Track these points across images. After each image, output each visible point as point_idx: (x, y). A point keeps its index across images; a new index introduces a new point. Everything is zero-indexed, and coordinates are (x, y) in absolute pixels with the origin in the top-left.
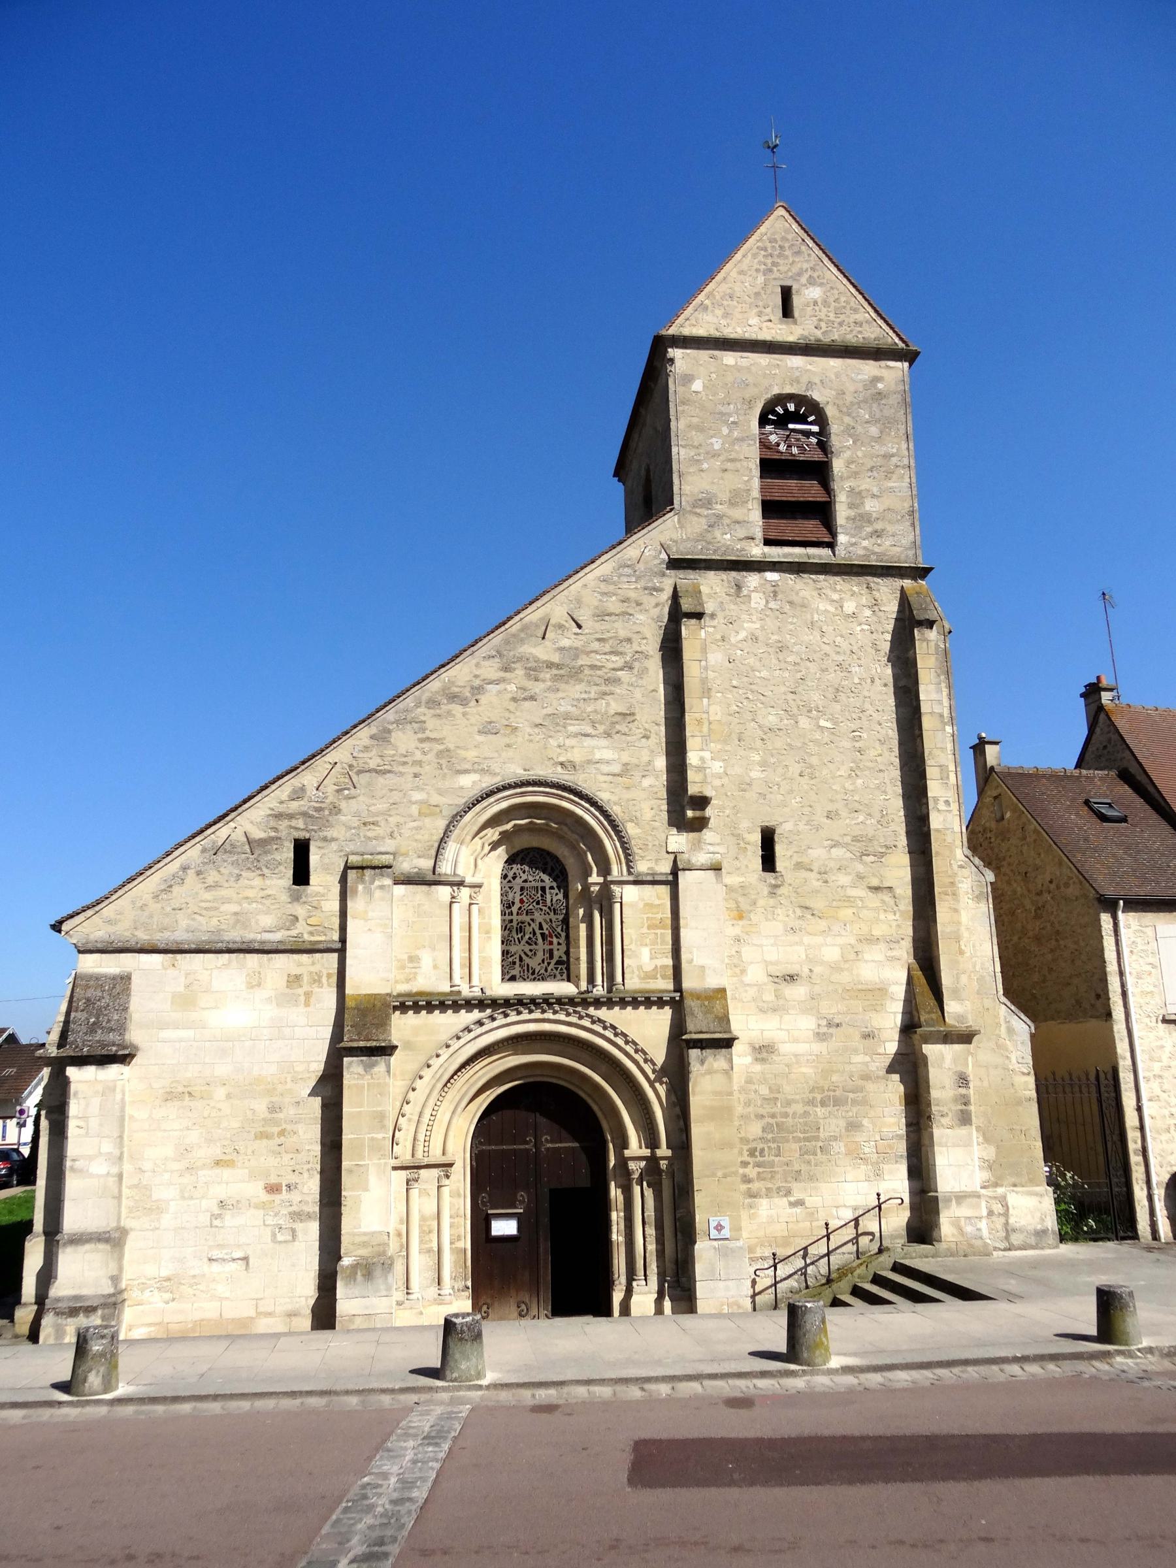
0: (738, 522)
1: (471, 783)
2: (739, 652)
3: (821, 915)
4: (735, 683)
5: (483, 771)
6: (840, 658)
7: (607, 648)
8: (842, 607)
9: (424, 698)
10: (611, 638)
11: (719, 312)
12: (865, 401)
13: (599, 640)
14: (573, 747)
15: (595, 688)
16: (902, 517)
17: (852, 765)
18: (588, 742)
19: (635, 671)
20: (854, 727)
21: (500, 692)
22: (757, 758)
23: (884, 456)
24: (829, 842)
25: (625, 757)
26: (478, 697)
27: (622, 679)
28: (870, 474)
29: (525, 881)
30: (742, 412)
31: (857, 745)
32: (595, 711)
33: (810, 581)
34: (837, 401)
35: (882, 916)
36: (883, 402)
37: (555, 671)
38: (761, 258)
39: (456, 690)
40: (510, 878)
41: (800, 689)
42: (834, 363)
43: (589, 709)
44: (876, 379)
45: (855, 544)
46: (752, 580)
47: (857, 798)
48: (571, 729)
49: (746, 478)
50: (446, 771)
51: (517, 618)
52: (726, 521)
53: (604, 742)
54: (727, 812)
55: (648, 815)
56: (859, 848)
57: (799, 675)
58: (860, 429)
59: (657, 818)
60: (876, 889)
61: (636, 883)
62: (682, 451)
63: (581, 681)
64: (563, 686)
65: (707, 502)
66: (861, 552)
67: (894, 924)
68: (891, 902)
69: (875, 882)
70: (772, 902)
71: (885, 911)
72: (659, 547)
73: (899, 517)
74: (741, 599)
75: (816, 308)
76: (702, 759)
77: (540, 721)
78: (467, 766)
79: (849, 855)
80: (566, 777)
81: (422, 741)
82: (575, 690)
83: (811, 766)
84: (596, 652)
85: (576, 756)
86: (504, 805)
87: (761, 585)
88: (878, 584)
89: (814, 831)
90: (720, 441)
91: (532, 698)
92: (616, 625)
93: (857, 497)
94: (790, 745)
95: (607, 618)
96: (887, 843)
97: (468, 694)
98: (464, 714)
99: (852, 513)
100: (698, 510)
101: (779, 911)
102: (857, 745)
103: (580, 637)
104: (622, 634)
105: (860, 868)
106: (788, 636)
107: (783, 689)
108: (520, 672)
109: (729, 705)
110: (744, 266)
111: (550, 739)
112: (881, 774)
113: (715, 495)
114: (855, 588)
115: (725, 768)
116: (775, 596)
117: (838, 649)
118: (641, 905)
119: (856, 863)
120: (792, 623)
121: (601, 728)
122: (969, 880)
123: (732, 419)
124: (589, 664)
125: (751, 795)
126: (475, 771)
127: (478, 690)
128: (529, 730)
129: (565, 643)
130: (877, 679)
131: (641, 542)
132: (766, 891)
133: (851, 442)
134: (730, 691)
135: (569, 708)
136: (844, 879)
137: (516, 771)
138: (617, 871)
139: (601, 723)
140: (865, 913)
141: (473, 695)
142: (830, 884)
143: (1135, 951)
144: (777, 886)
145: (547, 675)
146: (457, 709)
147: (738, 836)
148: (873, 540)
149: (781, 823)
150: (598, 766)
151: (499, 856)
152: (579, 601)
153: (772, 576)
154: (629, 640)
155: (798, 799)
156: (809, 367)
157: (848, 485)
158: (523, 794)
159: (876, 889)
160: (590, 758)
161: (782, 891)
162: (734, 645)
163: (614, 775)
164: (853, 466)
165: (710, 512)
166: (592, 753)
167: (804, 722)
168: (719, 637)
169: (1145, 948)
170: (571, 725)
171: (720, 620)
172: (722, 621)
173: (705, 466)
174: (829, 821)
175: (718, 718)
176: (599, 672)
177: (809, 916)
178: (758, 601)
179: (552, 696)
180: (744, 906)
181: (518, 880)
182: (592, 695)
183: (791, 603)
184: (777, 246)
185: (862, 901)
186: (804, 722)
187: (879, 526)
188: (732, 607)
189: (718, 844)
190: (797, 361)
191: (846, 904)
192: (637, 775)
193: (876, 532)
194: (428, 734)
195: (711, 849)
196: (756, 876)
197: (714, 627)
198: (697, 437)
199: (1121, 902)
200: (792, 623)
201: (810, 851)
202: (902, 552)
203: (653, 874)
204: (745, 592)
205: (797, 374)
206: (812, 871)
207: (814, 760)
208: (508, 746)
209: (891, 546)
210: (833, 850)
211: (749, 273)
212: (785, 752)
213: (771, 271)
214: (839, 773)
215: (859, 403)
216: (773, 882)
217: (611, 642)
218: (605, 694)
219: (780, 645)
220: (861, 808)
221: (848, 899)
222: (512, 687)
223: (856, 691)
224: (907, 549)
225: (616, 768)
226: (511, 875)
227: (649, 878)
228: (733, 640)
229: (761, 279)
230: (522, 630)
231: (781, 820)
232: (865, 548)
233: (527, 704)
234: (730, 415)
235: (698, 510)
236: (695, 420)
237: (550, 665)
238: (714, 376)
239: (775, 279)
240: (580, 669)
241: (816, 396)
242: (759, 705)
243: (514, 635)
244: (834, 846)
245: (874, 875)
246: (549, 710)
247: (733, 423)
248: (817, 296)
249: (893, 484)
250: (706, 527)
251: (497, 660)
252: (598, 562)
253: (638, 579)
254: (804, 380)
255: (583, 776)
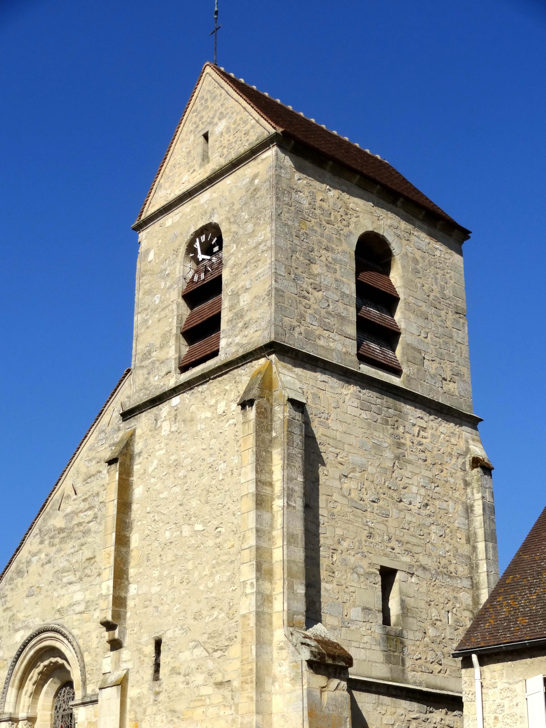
0: (163, 362)
1: (20, 637)
2: (153, 480)
3: (182, 717)
4: (148, 509)
5: (27, 627)
6: (210, 460)
7: (87, 507)
8: (216, 409)
9: (9, 578)
10: (89, 496)
11: (167, 185)
12: (246, 204)
13: (84, 500)
14: (64, 595)
15: (79, 541)
16: (263, 300)
17: (214, 562)
18: (72, 588)
19: (98, 520)
20: (216, 523)
21: (38, 561)
22: (156, 574)
23: (255, 248)
24: (193, 644)
25: (88, 597)
26: (28, 568)
27: (92, 530)
28: (245, 270)
29: (64, 710)
30: (172, 263)
31: (218, 541)
32: (77, 562)
33: (199, 395)
34: (229, 215)
35: (222, 713)
36: (257, 196)
37: (62, 535)
38: (194, 120)
39: (21, 566)
40: (58, 709)
41: (185, 501)
42: (228, 181)
43: (74, 561)
44: (255, 176)
45: (231, 343)
46: (164, 409)
47: (214, 595)
48: (65, 580)
49: (170, 320)
50: (11, 631)
51: (50, 498)
52: (157, 364)
53: (76, 587)
54: (136, 629)
55: (94, 642)
56: (213, 645)
57: (185, 487)
58: (241, 232)
59: (99, 645)
60: (219, 685)
61: (84, 704)
62: (139, 316)
63: (72, 538)
64: (63, 546)
65: (147, 355)
66: (233, 349)
67: (230, 718)
68: (228, 694)
69: (219, 678)
70: (155, 708)
71: (225, 706)
72: (120, 407)
73: (261, 302)
74: (157, 432)
75: (222, 139)
76: (108, 588)
77: (51, 579)
78: (20, 625)
79: (205, 653)
80: (59, 622)
81: (5, 610)
82: (69, 547)
83: (188, 572)
84: (81, 511)
85: (64, 603)
86: (32, 653)
87: (169, 412)
88: (240, 375)
89: (185, 634)
90: (159, 295)
91: (49, 562)
92: (94, 484)
93: (236, 295)
94: (176, 555)
95: (89, 480)
96: (231, 635)
97: (25, 568)
98: (22, 584)
99: (230, 315)
100: (143, 364)
101: (158, 718)
102: (218, 541)
103: (76, 502)
104: (96, 489)
105: (210, 665)
106: (181, 453)
107: (176, 503)
108: (47, 542)
109: (144, 530)
110: (183, 136)
111: (55, 593)
112: (232, 566)
113: (153, 345)
114: (227, 388)
115: (138, 589)
116: (176, 419)
117: (212, 452)
118: (86, 724)
119: (208, 661)
120: (184, 440)
121: (78, 574)
122: (287, 661)
123: (167, 273)
124: (77, 523)
125: (151, 609)
126: (22, 628)
127: (29, 562)
128: (46, 587)
129: (69, 510)
130: (235, 470)
131: (111, 407)
132: (152, 697)
133: (235, 247)
134: (145, 517)
135: (66, 564)
136: (199, 678)
137: (37, 623)
138: (79, 695)
139: (78, 571)
140: (212, 711)
141: (27, 567)
142: (191, 685)
143: (500, 717)
144: (157, 694)
145: (57, 541)
146: (19, 580)
147: (139, 651)
148: (242, 334)
149: (166, 632)
150: (74, 608)
151: (46, 692)
152: (78, 472)
153: (175, 401)
154: (98, 494)
155: (178, 606)
156: (215, 195)
157: (230, 290)
158: (41, 640)
159: (219, 685)
160: (71, 602)
161: (161, 697)
162: (150, 475)
163: (81, 613)
164: (234, 270)
165: (150, 361)
166: (72, 597)
167: (186, 530)
168: (142, 471)
169: (514, 710)
170: (65, 576)
171: (144, 455)
172: (146, 456)
173: (150, 322)
174: (195, 623)
175: (136, 545)
176: (81, 528)
177: (176, 720)
178: (166, 427)
179: (58, 556)
180: (140, 716)
181: (62, 709)
182: (76, 549)
183: (184, 421)
184: (203, 101)
185: (209, 698)
186: (186, 530)
187: (246, 319)
188: (152, 440)
189: (129, 660)
190: (205, 197)
191: (199, 703)
192: (92, 608)
193: (245, 324)
194: (8, 605)
195: (124, 666)
196: (147, 686)
197: (140, 463)
198: (147, 300)
199: (474, 657)
200: (184, 440)
201: (181, 654)
202: (260, 336)
203: (92, 695)
204: (159, 424)
205: (206, 206)
206: (180, 674)
207: (190, 565)
208: (37, 603)
209: (254, 333)
210: (195, 650)
211: (186, 138)
212: (173, 563)
213: (197, 127)
214: (205, 573)
215: (241, 208)
216: (157, 689)
217: (89, 499)
218: (82, 545)
219: (175, 463)
220: (216, 603)
221: (200, 698)
222: (43, 556)
223: (221, 487)
224: (266, 329)
225: (81, 608)
226: (58, 706)
227: (88, 700)
228: (150, 470)
229: (192, 137)
230: (51, 508)
231: (165, 629)
232: (238, 344)
233: (47, 567)
234: (165, 270)
235: (143, 364)
236: (147, 287)
237: (61, 530)
238: (160, 241)
239: (200, 131)
240: (73, 528)
241: (215, 220)
242: (161, 524)
243: (48, 513)
244: (195, 647)
245: (220, 671)
246: (56, 569)
247: (168, 275)
248: (222, 127)
249: (260, 271)
250: (146, 376)
251: (38, 536)
252: (89, 435)
253: (107, 438)
254: (210, 209)
255: (67, 618)
